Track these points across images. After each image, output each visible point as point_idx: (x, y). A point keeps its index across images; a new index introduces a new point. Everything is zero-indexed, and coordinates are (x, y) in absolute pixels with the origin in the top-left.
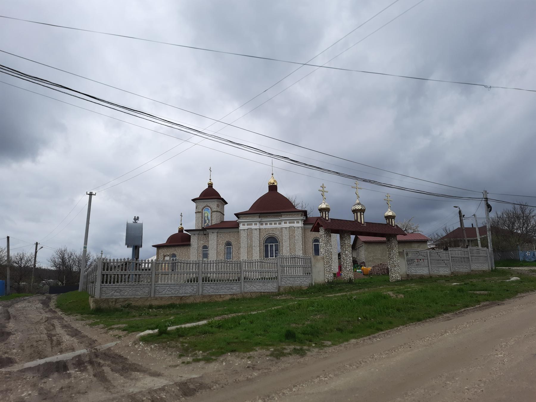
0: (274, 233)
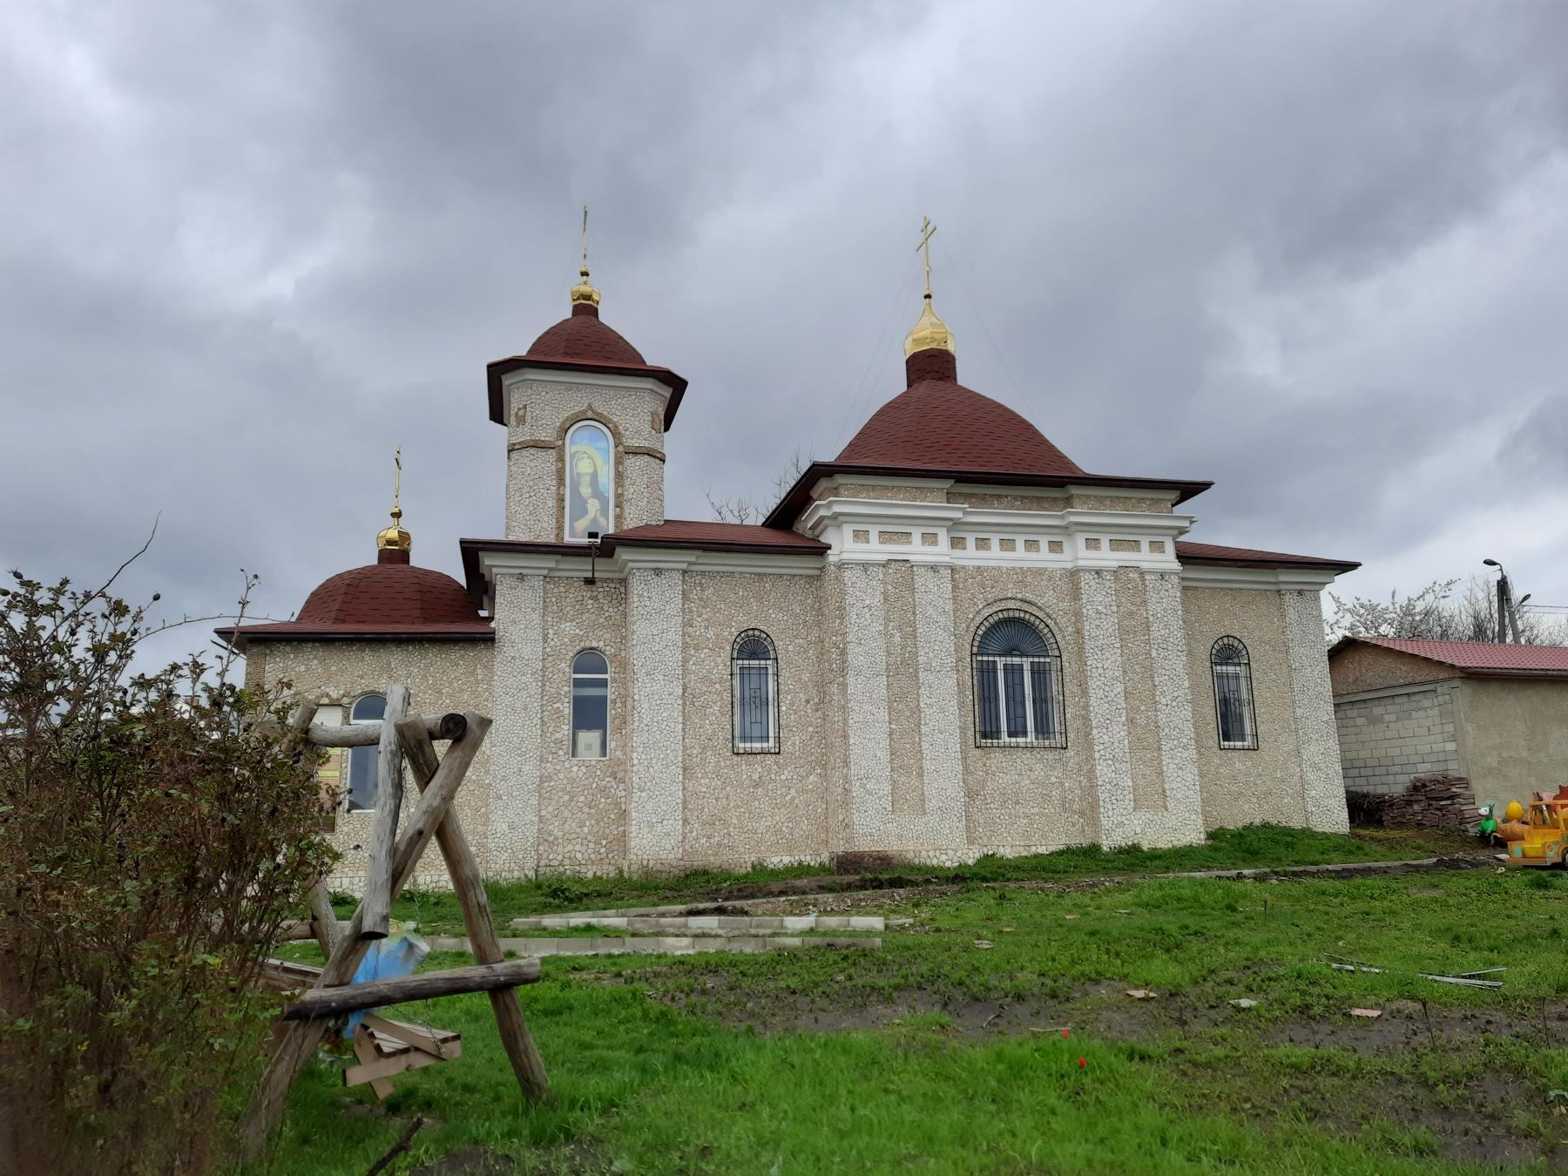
0: (1029, 597)
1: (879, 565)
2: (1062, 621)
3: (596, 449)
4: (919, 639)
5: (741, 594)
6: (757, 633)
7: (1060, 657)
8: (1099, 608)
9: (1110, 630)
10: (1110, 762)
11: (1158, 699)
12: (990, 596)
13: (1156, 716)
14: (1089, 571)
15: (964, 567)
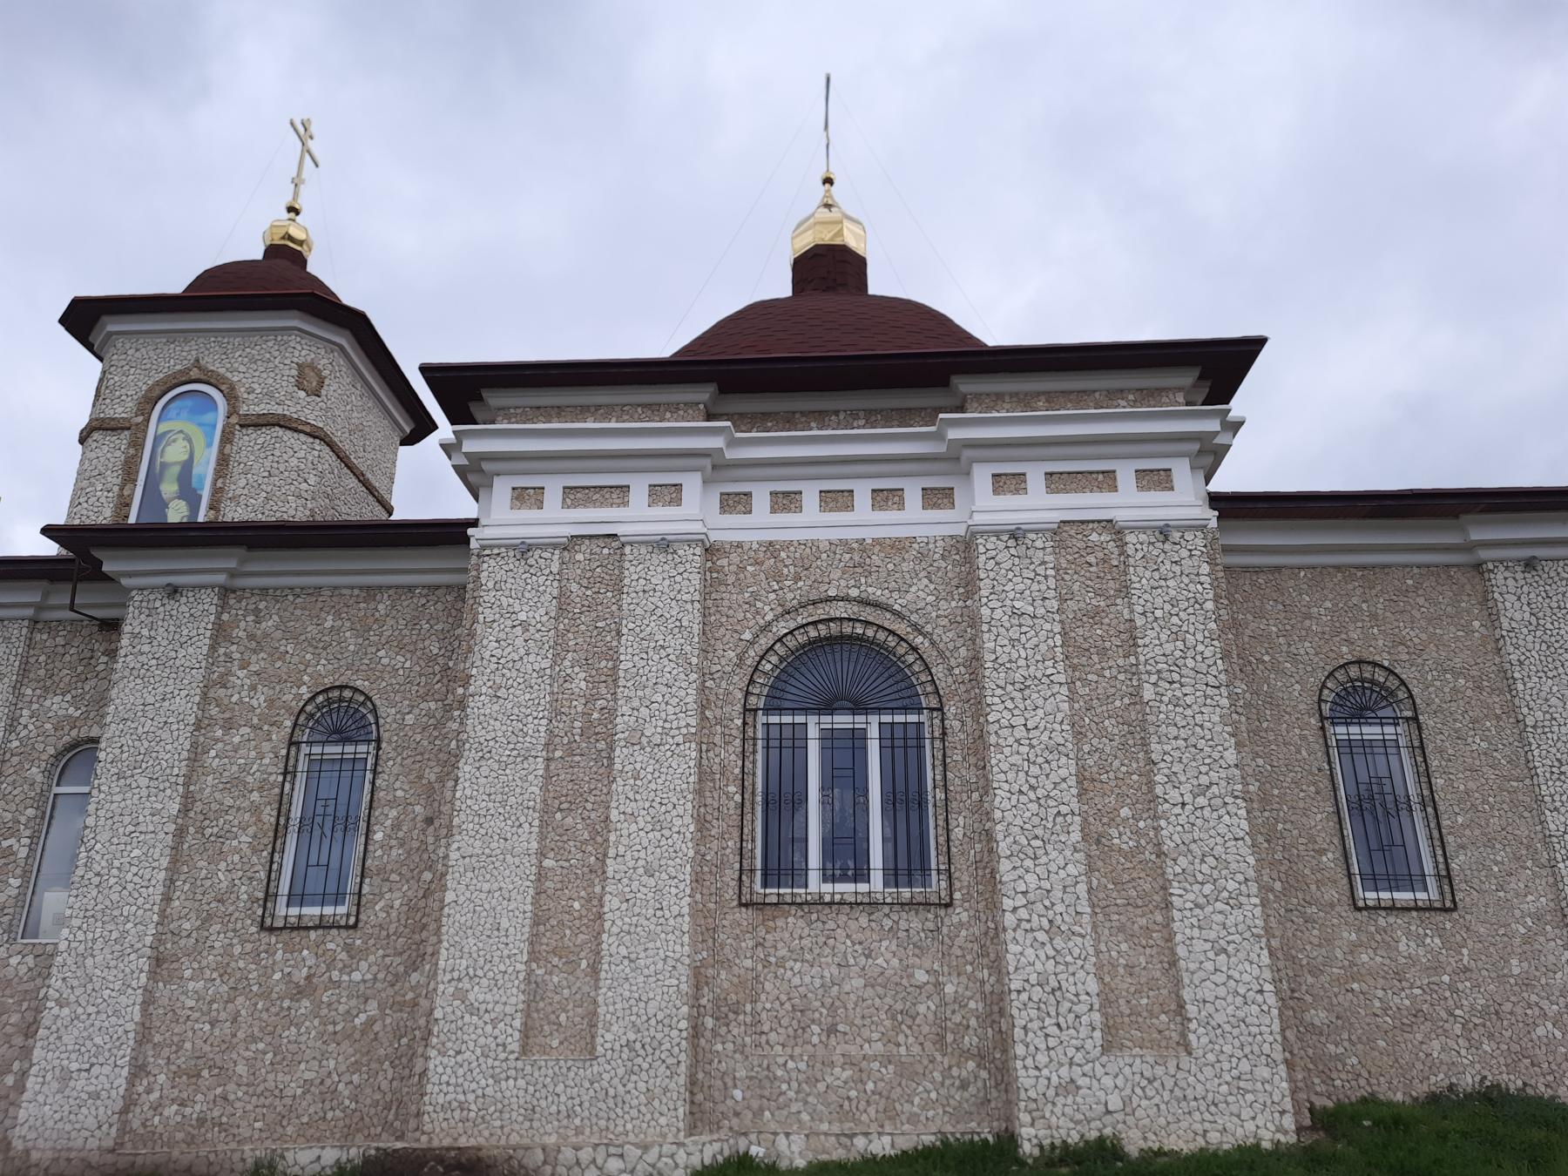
0: (875, 593)
1: (555, 546)
2: (946, 637)
3: (200, 425)
4: (621, 682)
5: (328, 624)
6: (347, 694)
7: (940, 709)
8: (1017, 604)
9: (1043, 647)
10: (1042, 936)
11: (1159, 790)
12: (790, 596)
13: (1157, 829)
14: (997, 534)
15: (739, 545)
